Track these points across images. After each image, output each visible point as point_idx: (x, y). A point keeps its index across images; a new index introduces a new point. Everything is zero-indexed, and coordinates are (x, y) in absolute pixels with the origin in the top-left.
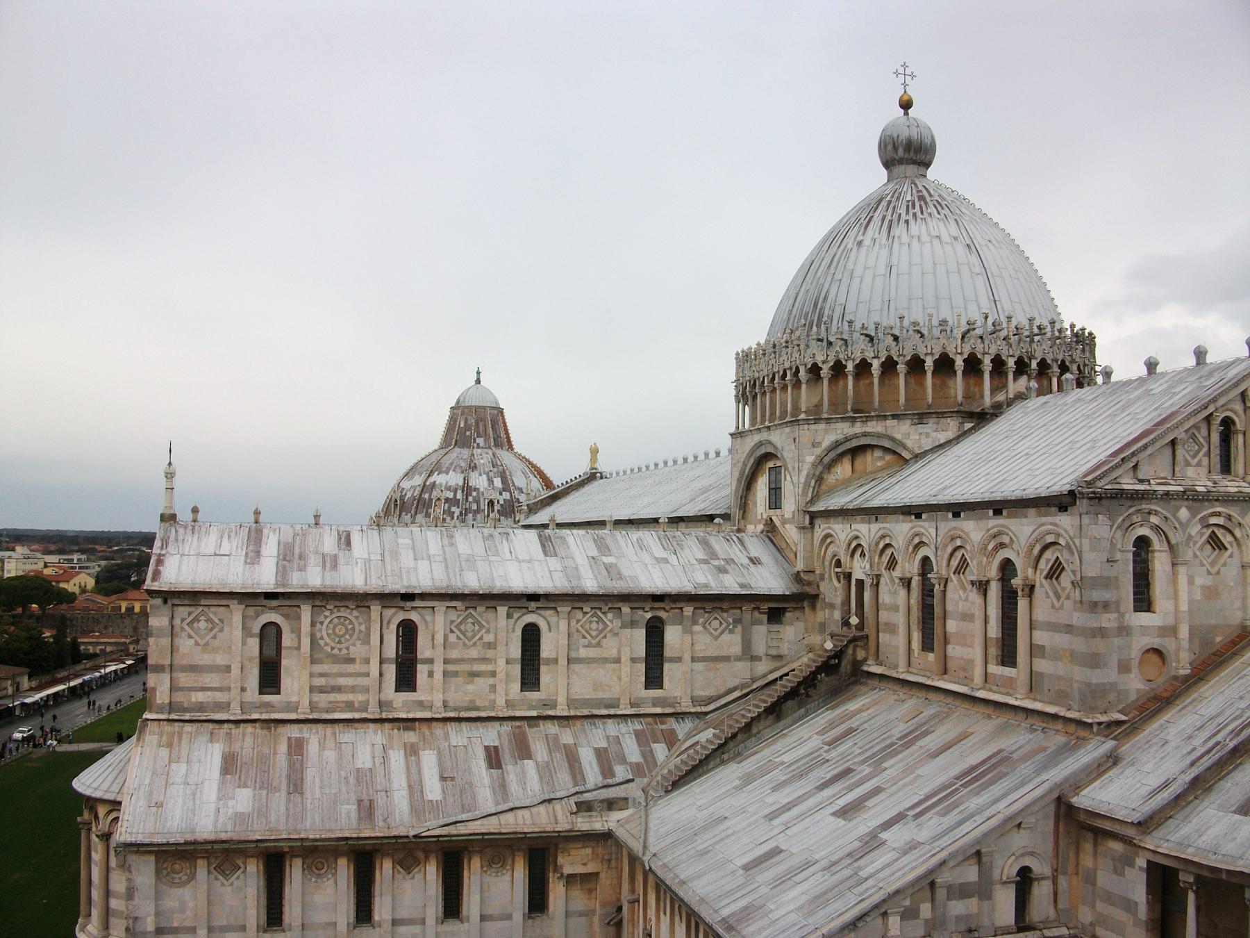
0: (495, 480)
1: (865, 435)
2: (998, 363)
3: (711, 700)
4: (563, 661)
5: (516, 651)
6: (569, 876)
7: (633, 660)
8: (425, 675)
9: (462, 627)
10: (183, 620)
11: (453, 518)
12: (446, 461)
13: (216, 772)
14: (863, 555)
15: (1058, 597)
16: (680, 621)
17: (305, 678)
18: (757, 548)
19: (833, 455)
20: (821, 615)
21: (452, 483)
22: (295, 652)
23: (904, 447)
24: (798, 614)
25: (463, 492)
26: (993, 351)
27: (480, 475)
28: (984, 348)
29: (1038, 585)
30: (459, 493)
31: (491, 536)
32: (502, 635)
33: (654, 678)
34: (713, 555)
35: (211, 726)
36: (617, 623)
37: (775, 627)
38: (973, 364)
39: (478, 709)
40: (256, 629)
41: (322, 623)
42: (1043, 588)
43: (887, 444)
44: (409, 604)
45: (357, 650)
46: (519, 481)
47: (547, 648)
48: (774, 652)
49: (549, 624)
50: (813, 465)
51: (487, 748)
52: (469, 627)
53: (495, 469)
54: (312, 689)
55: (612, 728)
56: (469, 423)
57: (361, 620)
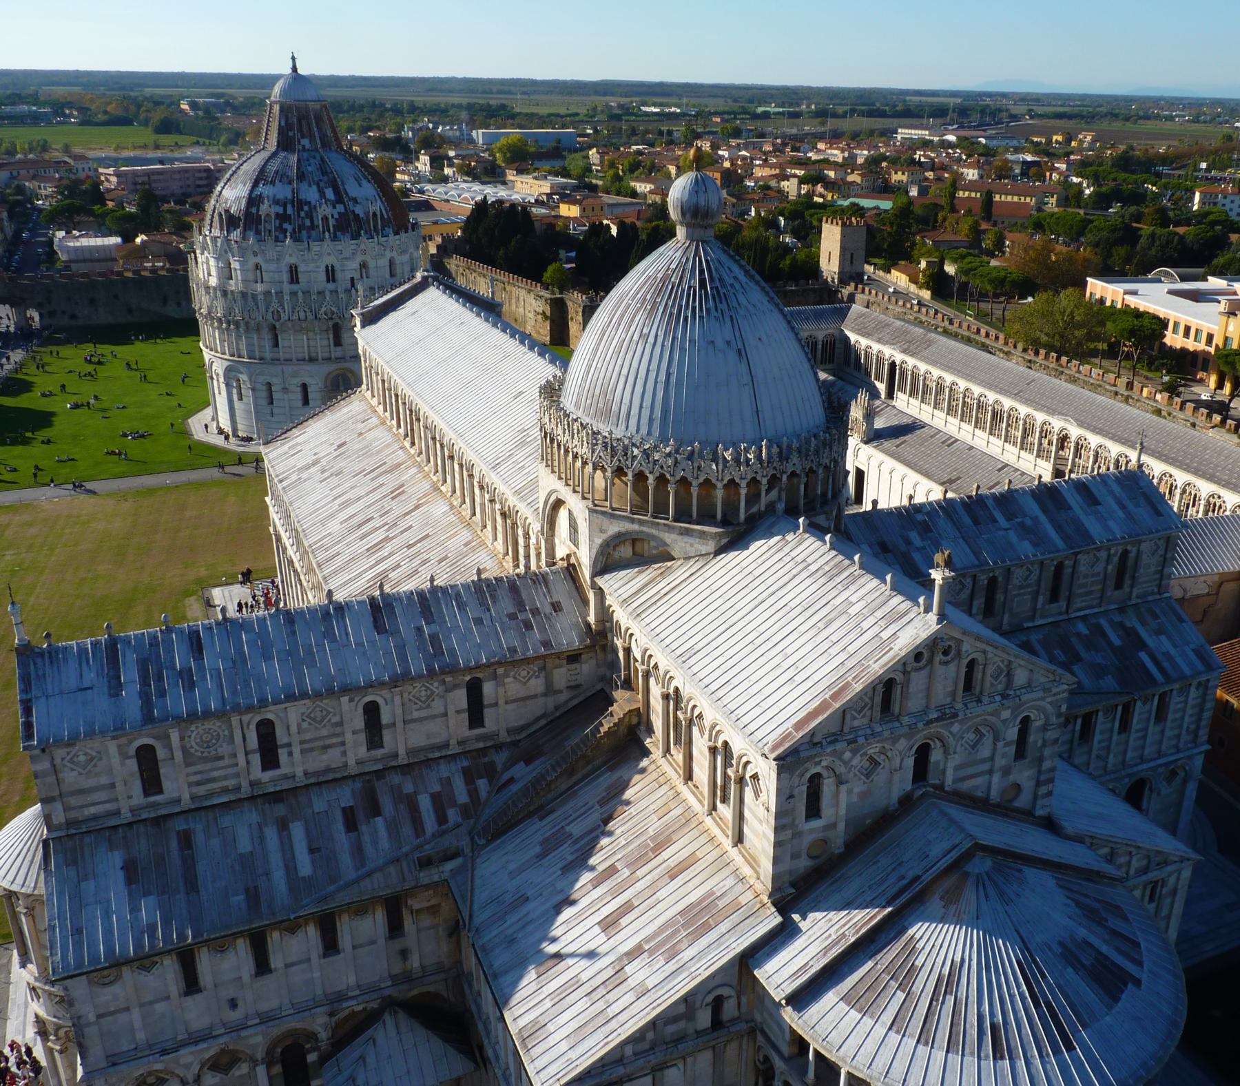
4: (400, 725)
5: (359, 722)
6: (418, 911)
7: (458, 712)
8: (286, 755)
11: (286, 237)
16: (495, 677)
21: (280, 196)
25: (293, 206)
27: (310, 186)
30: (289, 207)
36: (442, 688)
46: (352, 189)
47: (385, 718)
48: (572, 684)
51: (344, 810)
53: (325, 178)
55: (444, 770)
56: (290, 121)
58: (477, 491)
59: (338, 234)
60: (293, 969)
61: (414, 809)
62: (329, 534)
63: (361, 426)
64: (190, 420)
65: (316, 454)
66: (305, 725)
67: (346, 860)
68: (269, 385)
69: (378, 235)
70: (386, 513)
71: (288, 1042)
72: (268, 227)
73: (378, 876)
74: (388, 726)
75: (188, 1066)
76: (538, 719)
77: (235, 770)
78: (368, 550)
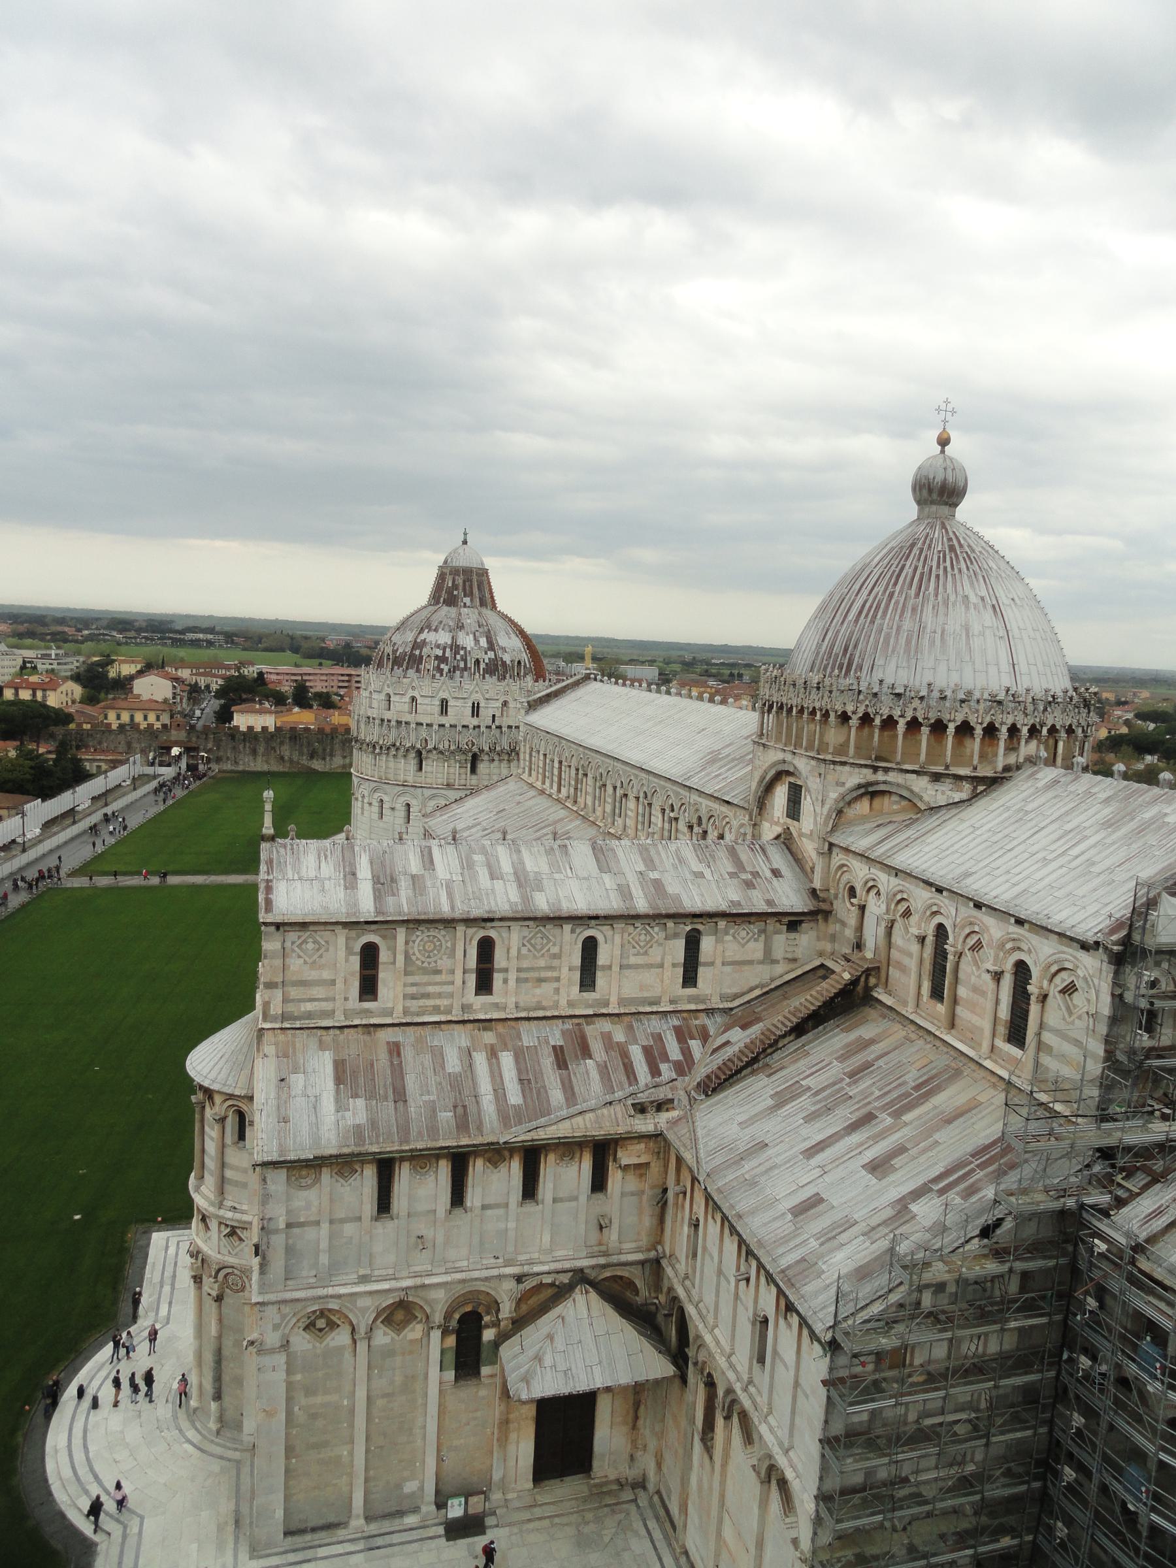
1: (885, 782)
2: (1013, 730)
3: (736, 996)
4: (616, 968)
5: (577, 960)
6: (625, 1168)
7: (674, 965)
8: (501, 982)
10: (293, 943)
11: (442, 675)
13: (330, 1084)
14: (878, 893)
15: (1070, 1013)
16: (715, 932)
18: (779, 859)
19: (855, 794)
20: (833, 927)
21: (441, 642)
23: (921, 798)
24: (812, 924)
26: (1010, 721)
29: (1051, 994)
30: (448, 650)
31: (552, 849)
32: (566, 948)
33: (690, 978)
35: (319, 1032)
36: (662, 935)
37: (792, 935)
38: (991, 731)
39: (544, 1008)
40: (358, 948)
41: (414, 942)
42: (1055, 1000)
43: (905, 793)
44: (489, 924)
45: (444, 963)
47: (602, 959)
48: (790, 956)
50: (836, 801)
52: (539, 941)
54: (405, 996)
55: (655, 1024)
59: (487, 676)
60: (489, 1212)
63: (518, 798)
66: (524, 951)
67: (556, 1095)
68: (408, 805)
71: (468, 1308)
72: (428, 667)
73: (589, 1116)
74: (604, 968)
75: (364, 1310)
76: (752, 989)
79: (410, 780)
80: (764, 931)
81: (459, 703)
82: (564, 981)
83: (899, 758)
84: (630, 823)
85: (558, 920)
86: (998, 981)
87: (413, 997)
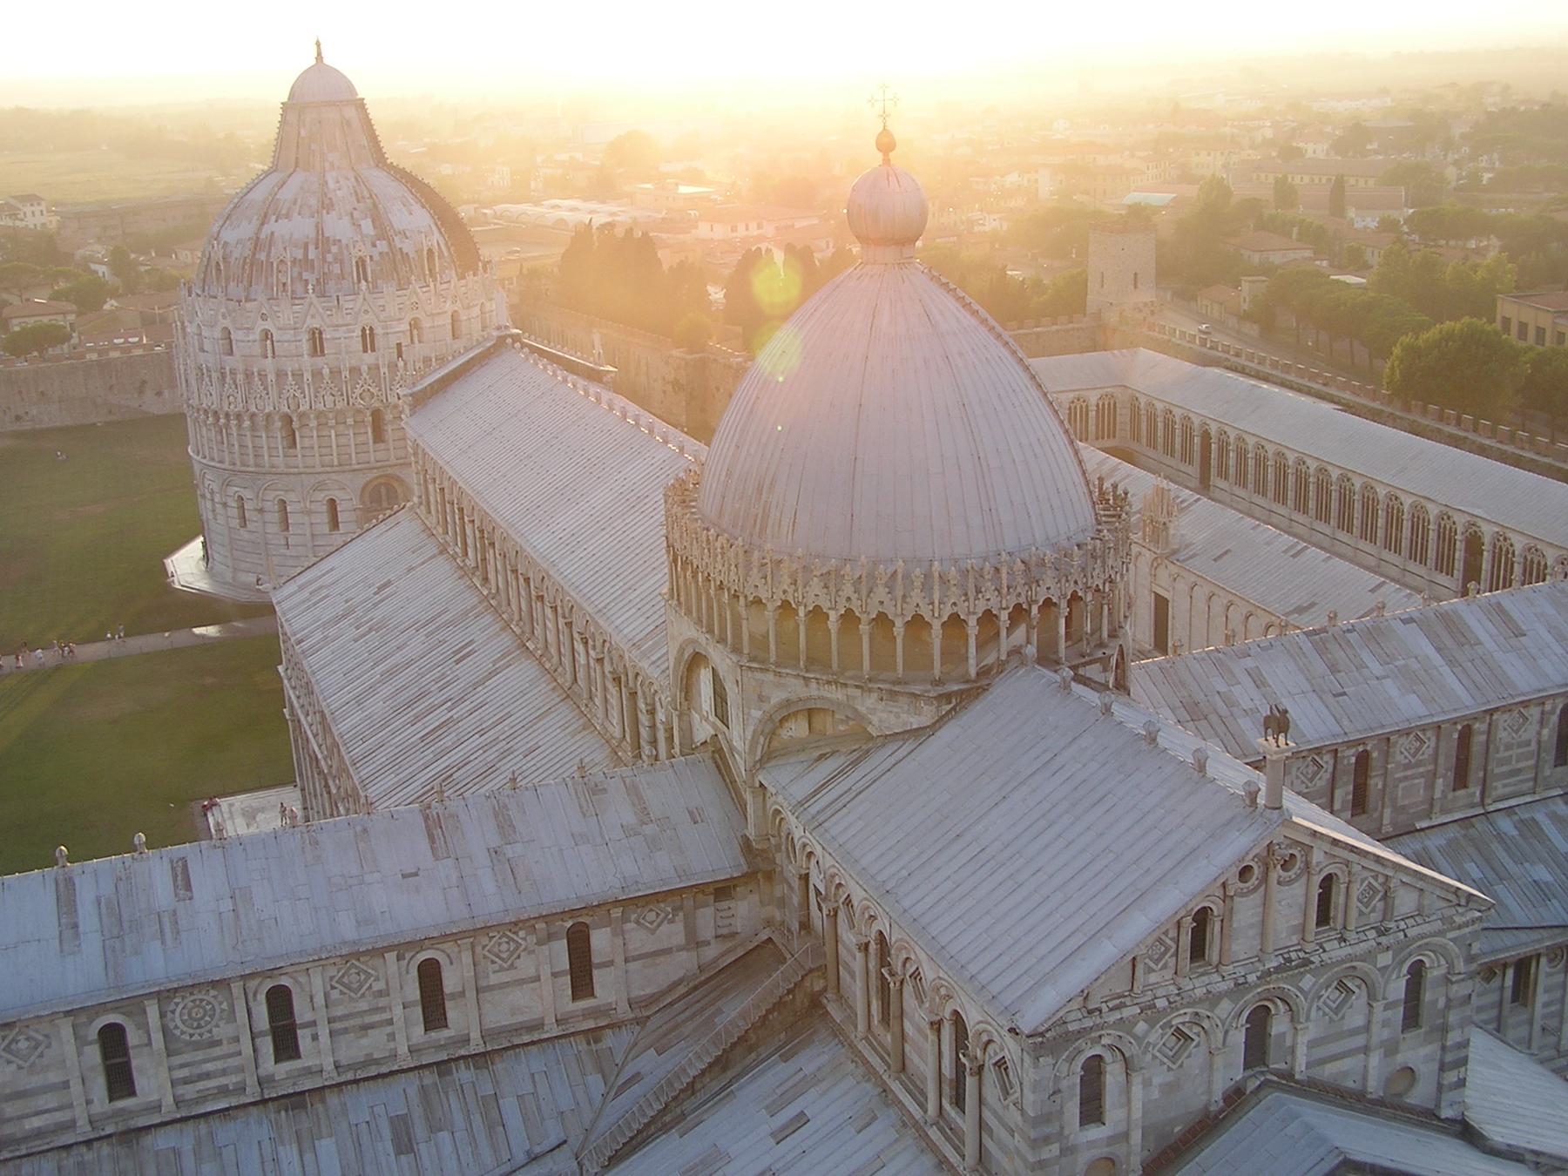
0: (363, 223)
4: (471, 994)
5: (413, 992)
7: (555, 975)
9: (345, 980)
12: (286, 194)
15: (1006, 1094)
17: (164, 1075)
20: (780, 890)
22: (146, 1050)
25: (317, 248)
26: (981, 607)
28: (968, 607)
29: (986, 1065)
30: (311, 248)
32: (395, 983)
34: (644, 813)
37: (724, 905)
40: (93, 1032)
41: (173, 1012)
42: (990, 1075)
44: (275, 972)
45: (223, 1031)
47: (450, 982)
48: (725, 931)
49: (449, 956)
51: (393, 1121)
57: (220, 998)
58: (579, 647)
61: (495, 1123)
62: (368, 717)
64: (168, 562)
65: (347, 602)
69: (435, 280)
70: (448, 684)
74: (453, 996)
77: (232, 1062)
78: (422, 739)
79: (280, 461)
80: (681, 908)
81: (341, 333)
82: (399, 1023)
83: (835, 666)
84: (551, 638)
85: (380, 952)
86: (939, 1030)
87: (186, 1081)
